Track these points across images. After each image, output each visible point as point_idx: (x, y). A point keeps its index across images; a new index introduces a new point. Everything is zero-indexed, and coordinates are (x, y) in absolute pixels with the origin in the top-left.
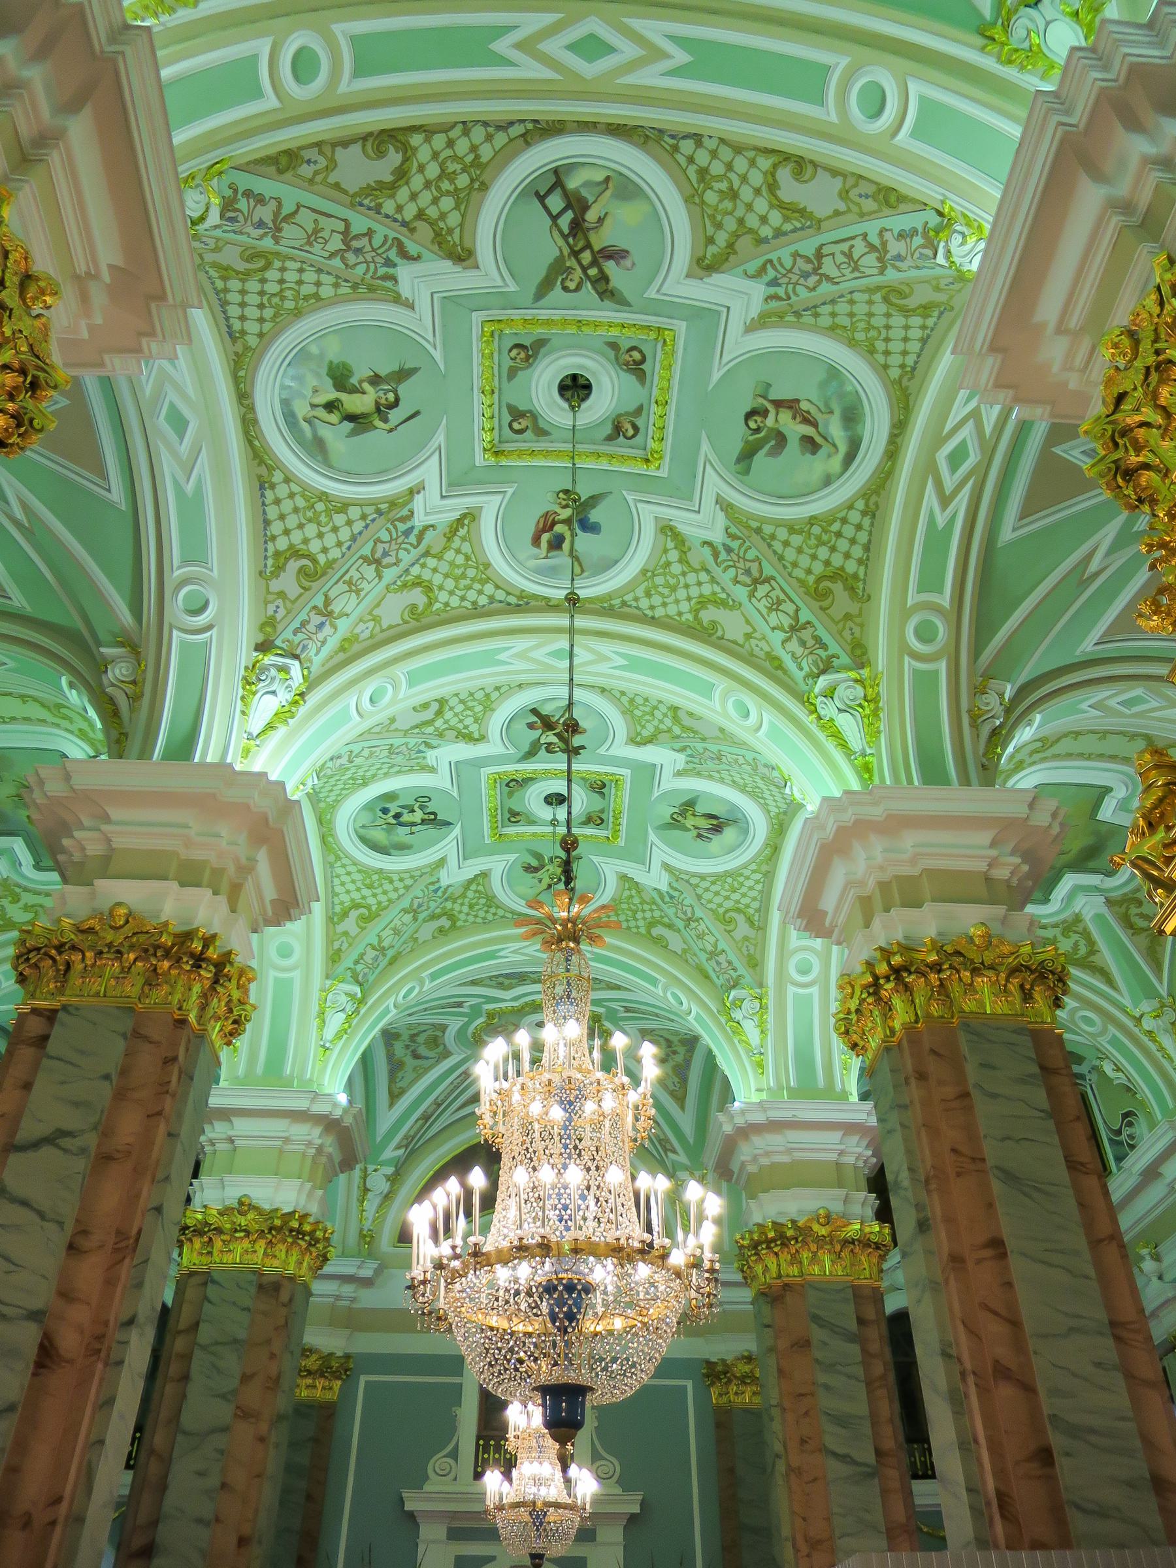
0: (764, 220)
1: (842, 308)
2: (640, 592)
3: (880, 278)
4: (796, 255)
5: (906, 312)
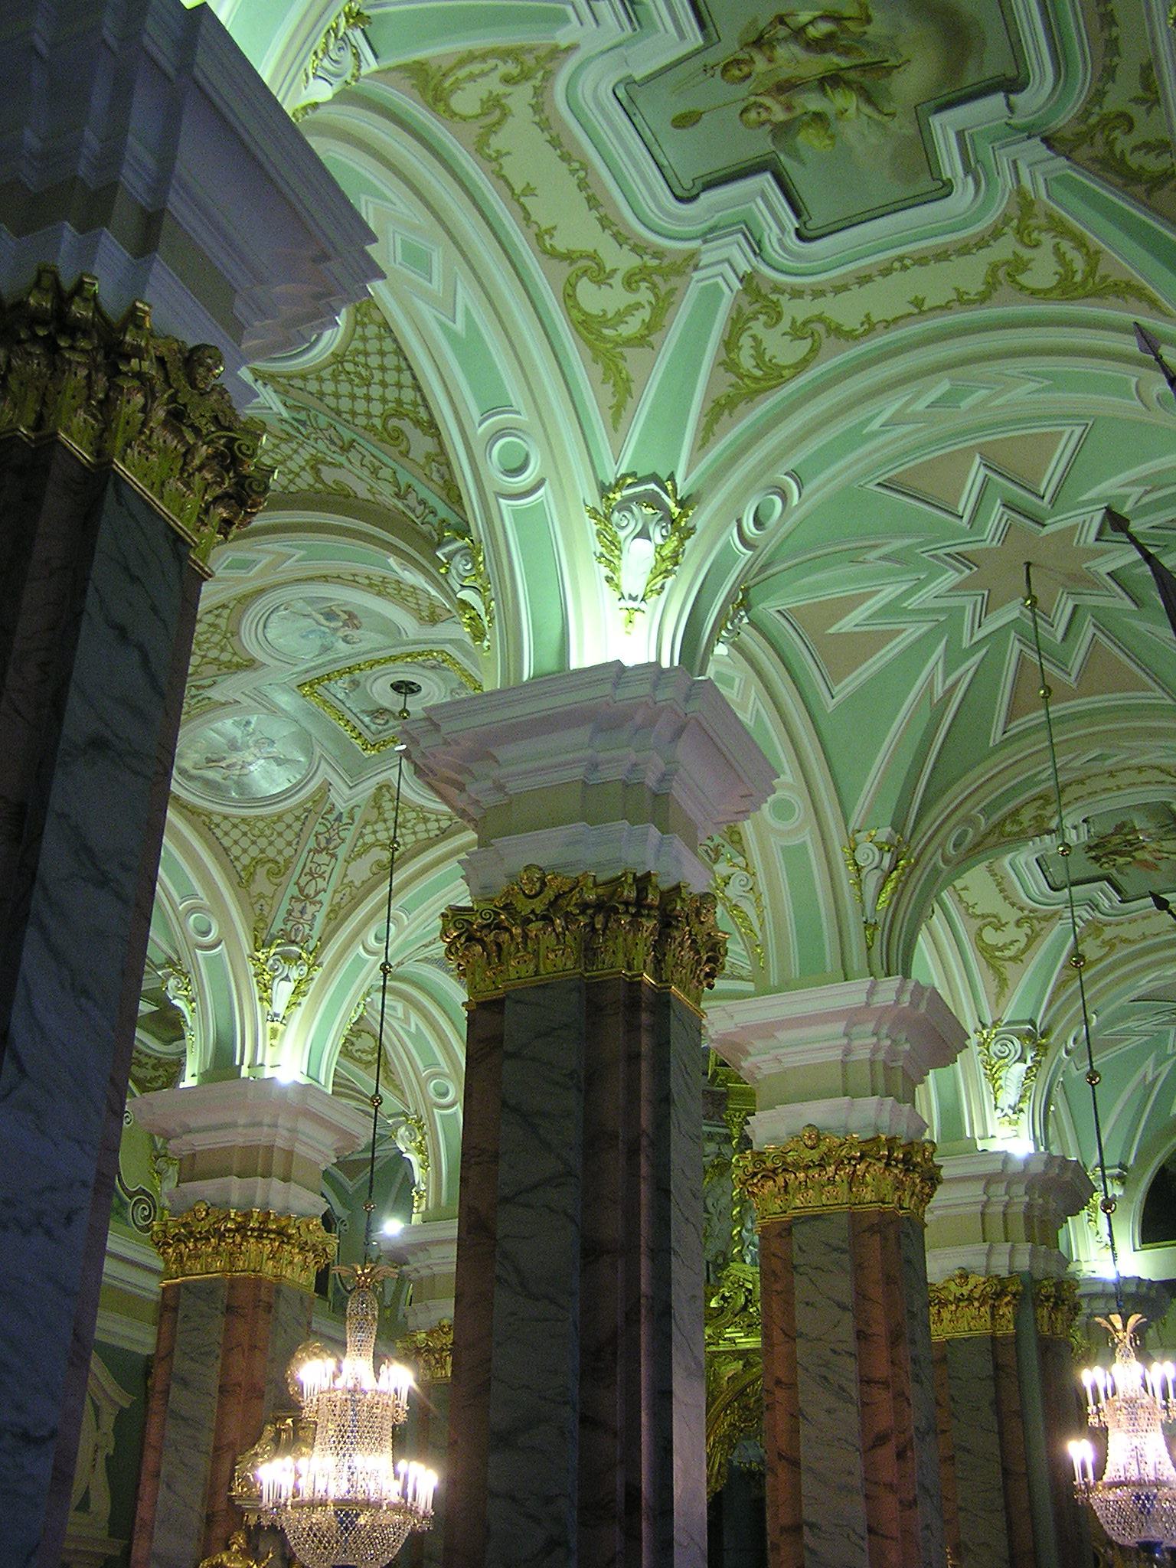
0: (375, 832)
1: (289, 835)
2: (222, 622)
3: (294, 879)
4: (343, 840)
5: (258, 862)
